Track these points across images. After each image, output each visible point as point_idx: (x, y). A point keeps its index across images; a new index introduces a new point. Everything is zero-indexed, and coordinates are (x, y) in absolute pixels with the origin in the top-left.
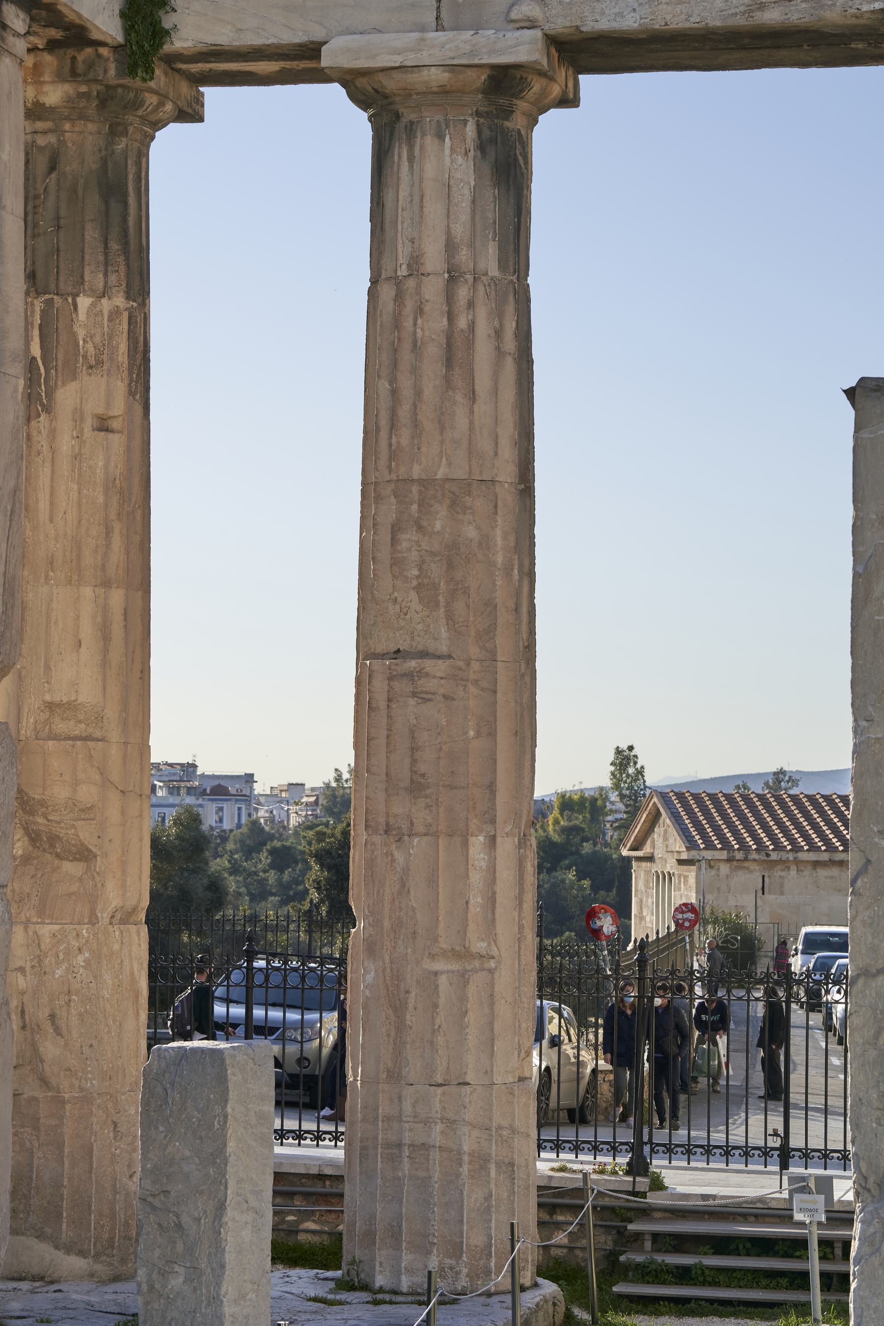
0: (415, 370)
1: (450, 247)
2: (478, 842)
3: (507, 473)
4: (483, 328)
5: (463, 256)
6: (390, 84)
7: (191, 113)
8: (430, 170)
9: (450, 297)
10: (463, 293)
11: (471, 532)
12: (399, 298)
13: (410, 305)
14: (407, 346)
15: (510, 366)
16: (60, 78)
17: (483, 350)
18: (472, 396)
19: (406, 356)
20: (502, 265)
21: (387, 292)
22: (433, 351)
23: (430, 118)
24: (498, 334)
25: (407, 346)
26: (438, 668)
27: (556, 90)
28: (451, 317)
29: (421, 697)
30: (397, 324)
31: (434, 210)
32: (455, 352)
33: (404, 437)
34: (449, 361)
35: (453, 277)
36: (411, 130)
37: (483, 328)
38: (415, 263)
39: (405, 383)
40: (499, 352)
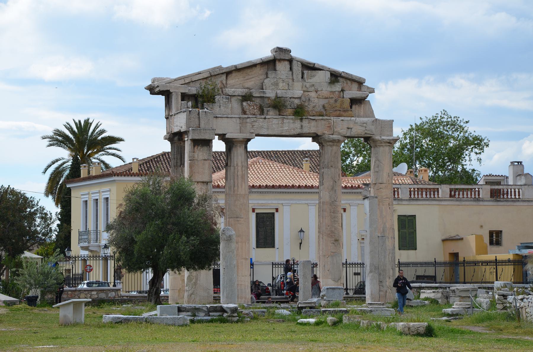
0: (238, 179)
5: (243, 163)
6: (234, 140)
8: (239, 151)
10: (243, 169)
13: (236, 170)
14: (236, 176)
19: (236, 177)
23: (239, 145)
25: (236, 176)
30: (234, 172)
31: (240, 157)
33: (236, 188)
36: (236, 146)
38: (237, 165)
39: (236, 181)
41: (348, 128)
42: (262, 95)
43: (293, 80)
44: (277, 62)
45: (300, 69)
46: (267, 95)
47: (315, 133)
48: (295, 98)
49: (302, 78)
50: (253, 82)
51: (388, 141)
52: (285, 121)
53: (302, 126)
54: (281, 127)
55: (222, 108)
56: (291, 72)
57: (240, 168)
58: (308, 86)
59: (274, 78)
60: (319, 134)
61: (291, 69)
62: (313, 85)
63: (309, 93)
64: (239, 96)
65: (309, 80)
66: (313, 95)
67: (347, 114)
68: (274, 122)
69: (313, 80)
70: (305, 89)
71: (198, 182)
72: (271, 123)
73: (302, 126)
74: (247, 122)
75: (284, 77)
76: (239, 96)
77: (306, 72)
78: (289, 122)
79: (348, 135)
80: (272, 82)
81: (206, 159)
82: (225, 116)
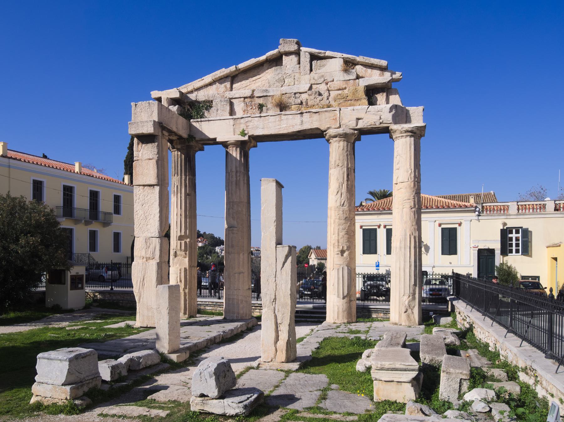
1: (236, 167)
2: (241, 255)
3: (245, 200)
4: (241, 179)
5: (238, 169)
7: (202, 149)
9: (236, 175)
10: (238, 174)
11: (240, 209)
12: (229, 175)
15: (246, 185)
16: (180, 144)
17: (242, 183)
18: (240, 189)
20: (244, 170)
21: (228, 174)
22: (234, 183)
24: (244, 180)
26: (235, 229)
27: (252, 145)
28: (236, 178)
29: (233, 233)
30: (229, 179)
32: (237, 183)
34: (236, 184)
35: (237, 172)
37: (241, 179)
38: (231, 170)
39: (230, 187)
40: (244, 183)
41: (358, 119)
42: (265, 94)
43: (300, 73)
44: (284, 56)
45: (308, 60)
46: (271, 94)
47: (318, 129)
48: (300, 93)
49: (311, 70)
50: (260, 83)
51: (410, 129)
52: (283, 117)
53: (302, 122)
54: (278, 125)
55: (219, 111)
56: (298, 66)
57: (234, 174)
58: (316, 78)
59: (278, 74)
60: (323, 128)
61: (299, 63)
62: (323, 76)
63: (318, 86)
64: (240, 98)
65: (318, 71)
66: (322, 88)
67: (359, 102)
68: (270, 120)
69: (322, 71)
70: (313, 82)
71: (144, 186)
72: (267, 122)
73: (302, 122)
74: (241, 123)
75: (290, 72)
76: (240, 98)
77: (314, 63)
78: (287, 119)
79: (358, 127)
80: (277, 78)
81: (151, 157)
82: (218, 118)
